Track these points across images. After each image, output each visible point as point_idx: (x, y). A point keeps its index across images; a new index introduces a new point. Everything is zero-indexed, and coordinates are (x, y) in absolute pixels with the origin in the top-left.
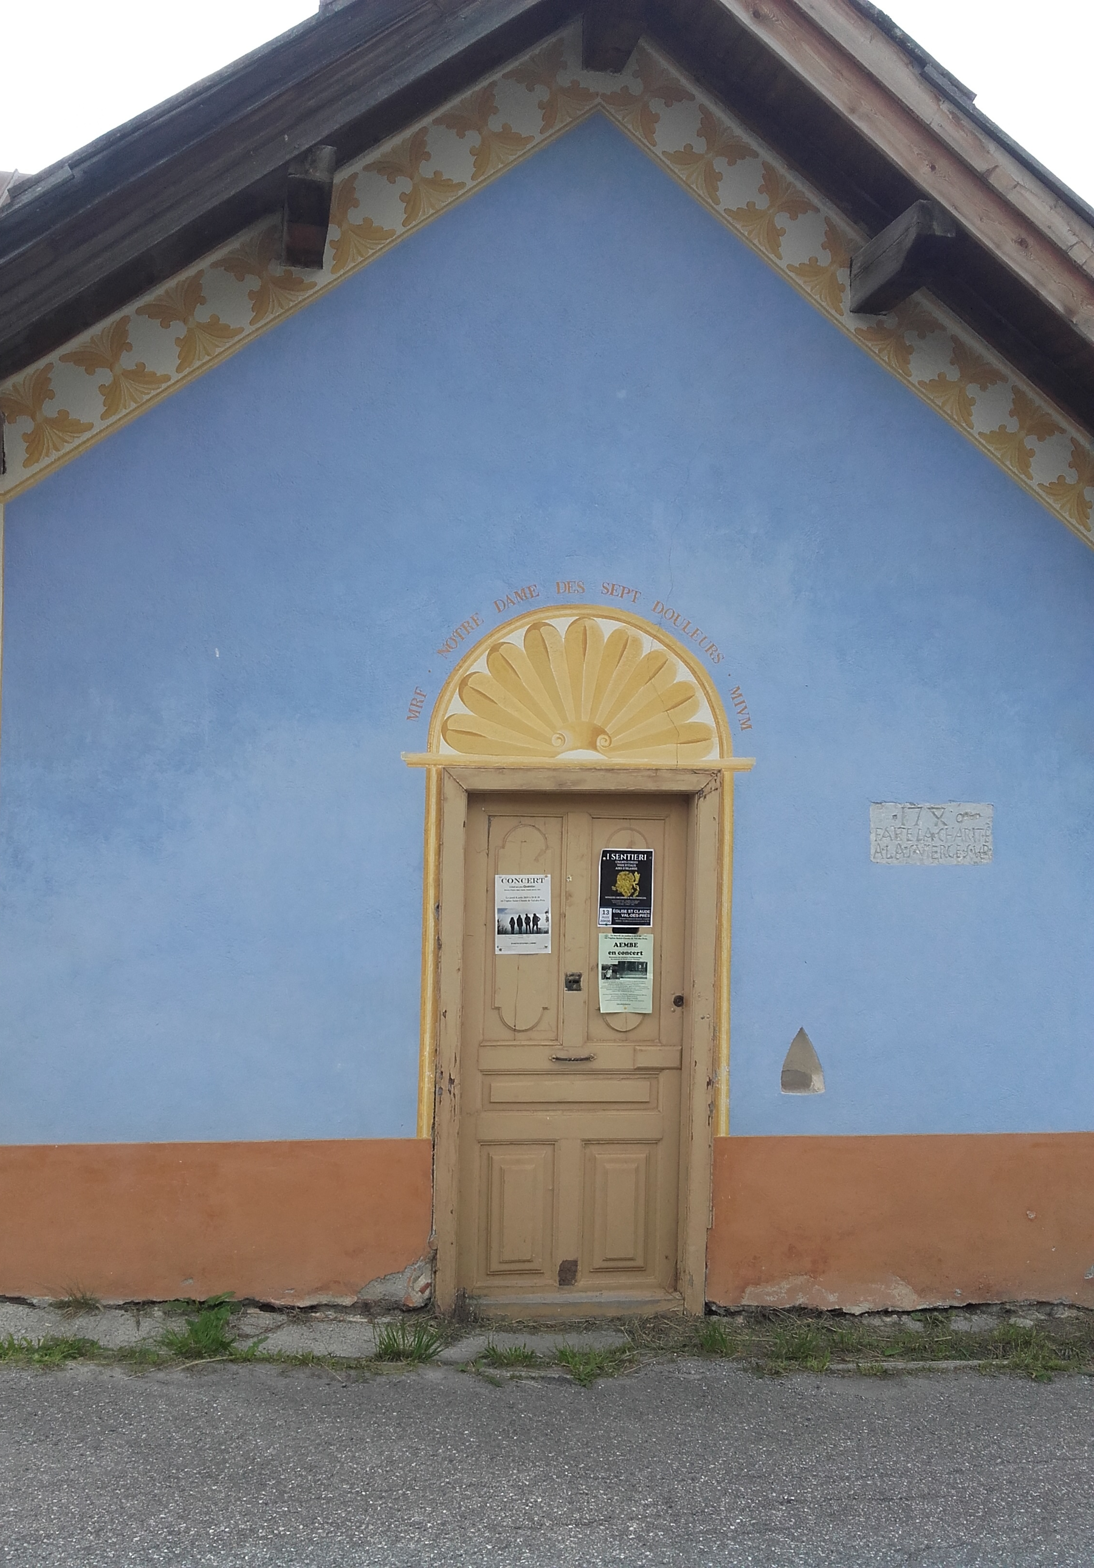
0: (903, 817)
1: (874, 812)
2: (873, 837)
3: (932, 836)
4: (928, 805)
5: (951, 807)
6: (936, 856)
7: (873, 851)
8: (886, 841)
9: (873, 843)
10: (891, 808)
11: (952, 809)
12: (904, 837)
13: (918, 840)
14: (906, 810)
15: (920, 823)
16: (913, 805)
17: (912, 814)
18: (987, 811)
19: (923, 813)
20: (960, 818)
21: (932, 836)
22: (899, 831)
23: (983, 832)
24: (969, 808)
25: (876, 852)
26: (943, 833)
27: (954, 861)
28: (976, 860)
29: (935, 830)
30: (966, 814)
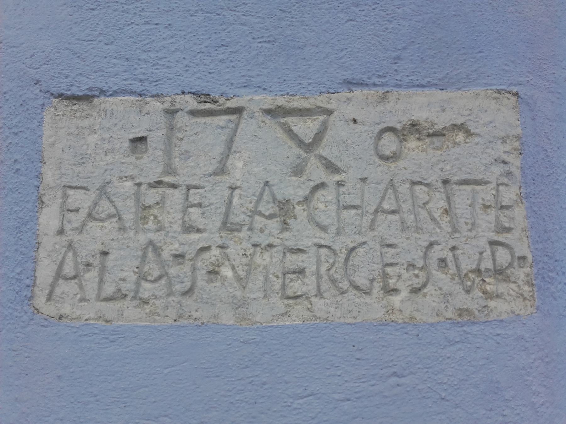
0: (169, 142)
1: (58, 129)
2: (49, 219)
3: (284, 210)
4: (266, 100)
5: (350, 106)
6: (296, 287)
7: (45, 272)
8: (99, 234)
9: (49, 242)
10: (123, 116)
11: (354, 118)
12: (172, 216)
13: (228, 226)
14: (182, 119)
15: (237, 164)
16: (208, 105)
17: (209, 133)
18: (496, 117)
19: (248, 127)
20: (389, 144)
21: (284, 210)
22: (151, 196)
23: (486, 194)
24: (421, 106)
25: (59, 275)
26: (325, 200)
27: (373, 308)
28: (461, 300)
29: (293, 189)
30: (414, 126)
